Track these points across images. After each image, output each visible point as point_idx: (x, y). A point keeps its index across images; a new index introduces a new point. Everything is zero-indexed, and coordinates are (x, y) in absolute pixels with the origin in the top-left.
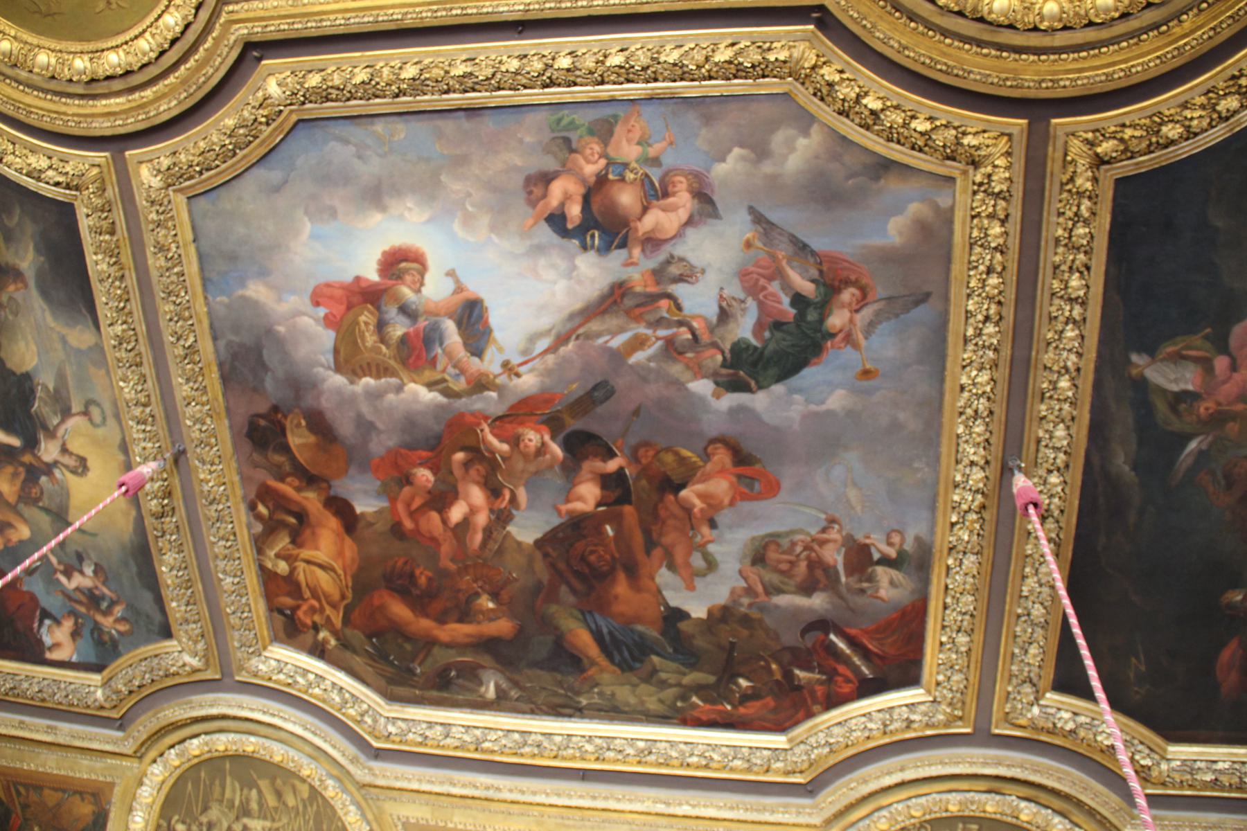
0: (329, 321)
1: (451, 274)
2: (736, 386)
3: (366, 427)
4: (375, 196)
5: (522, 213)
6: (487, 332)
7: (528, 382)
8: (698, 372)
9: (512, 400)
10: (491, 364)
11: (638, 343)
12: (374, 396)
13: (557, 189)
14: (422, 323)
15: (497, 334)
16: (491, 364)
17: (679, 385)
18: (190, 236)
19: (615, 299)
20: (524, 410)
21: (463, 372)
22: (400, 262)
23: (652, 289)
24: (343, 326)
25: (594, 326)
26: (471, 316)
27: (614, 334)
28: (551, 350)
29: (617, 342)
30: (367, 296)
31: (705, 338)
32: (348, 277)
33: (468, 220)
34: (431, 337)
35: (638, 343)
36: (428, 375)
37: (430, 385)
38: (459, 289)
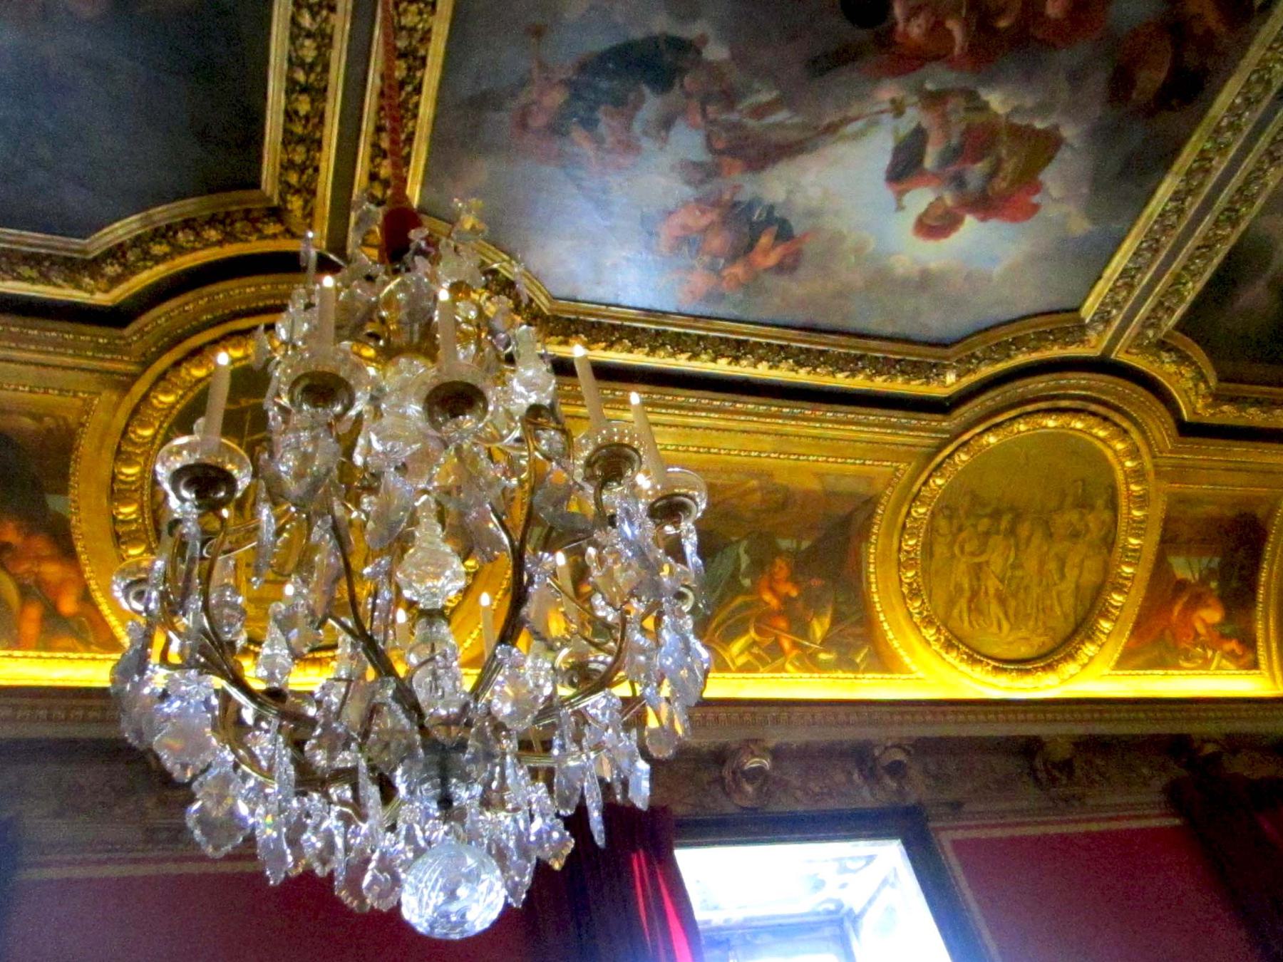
0: (1037, 188)
1: (900, 208)
2: (681, 46)
3: (1076, 78)
4: (925, 281)
5: (811, 248)
6: (897, 151)
7: (888, 91)
8: (714, 70)
9: (914, 78)
10: (913, 117)
11: (759, 111)
12: (1043, 109)
13: (772, 259)
14: (952, 169)
15: (890, 145)
16: (913, 117)
17: (739, 57)
18: (1101, 283)
19: (764, 154)
20: (906, 61)
21: (944, 116)
22: (935, 225)
23: (727, 160)
24: (1028, 179)
25: (794, 135)
26: (905, 168)
27: (781, 125)
28: (847, 121)
29: (782, 116)
30: (985, 205)
31: (695, 103)
32: (993, 223)
33: (858, 250)
34: (956, 155)
35: (759, 111)
36: (978, 118)
37: (985, 107)
38: (900, 194)
